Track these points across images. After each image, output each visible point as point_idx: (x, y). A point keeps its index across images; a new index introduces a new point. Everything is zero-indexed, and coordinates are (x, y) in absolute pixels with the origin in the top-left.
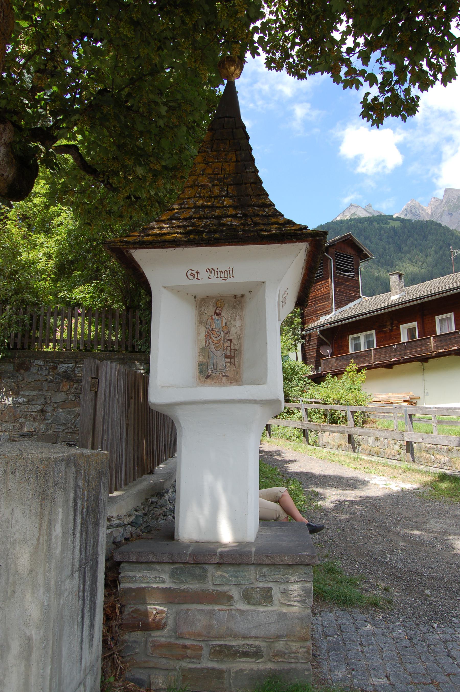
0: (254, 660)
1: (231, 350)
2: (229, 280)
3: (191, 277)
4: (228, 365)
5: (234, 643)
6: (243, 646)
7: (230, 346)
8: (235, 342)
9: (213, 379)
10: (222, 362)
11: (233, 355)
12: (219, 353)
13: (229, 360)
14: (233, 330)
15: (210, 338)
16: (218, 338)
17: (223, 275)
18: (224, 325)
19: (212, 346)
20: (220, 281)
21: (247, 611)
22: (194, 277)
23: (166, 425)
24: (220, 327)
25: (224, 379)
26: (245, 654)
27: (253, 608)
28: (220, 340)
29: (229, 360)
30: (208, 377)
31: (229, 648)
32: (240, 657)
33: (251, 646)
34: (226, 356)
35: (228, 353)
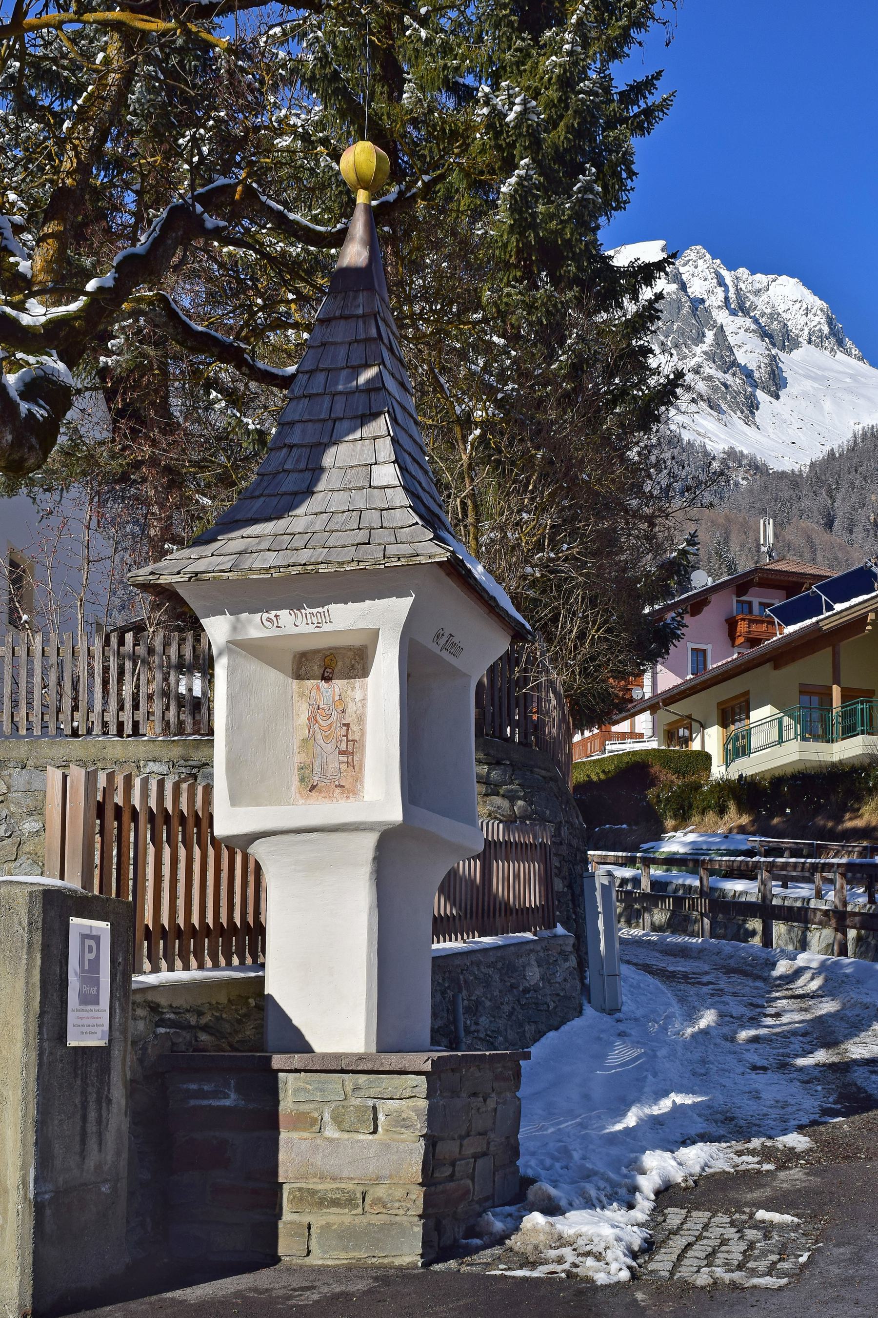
0: (346, 1211)
1: (348, 741)
2: (326, 628)
3: (267, 623)
4: (344, 767)
5: (320, 1187)
6: (332, 1190)
7: (347, 736)
8: (354, 727)
9: (320, 792)
10: (334, 762)
11: (350, 750)
12: (329, 748)
13: (345, 759)
14: (351, 708)
15: (316, 721)
16: (329, 722)
17: (315, 620)
18: (337, 698)
19: (319, 736)
20: (311, 629)
21: (338, 1139)
22: (272, 623)
23: (251, 879)
24: (331, 702)
25: (338, 790)
26: (335, 1203)
27: (346, 1135)
28: (331, 725)
29: (345, 759)
30: (313, 788)
31: (312, 1192)
32: (328, 1207)
33: (343, 1190)
34: (341, 753)
35: (343, 747)
